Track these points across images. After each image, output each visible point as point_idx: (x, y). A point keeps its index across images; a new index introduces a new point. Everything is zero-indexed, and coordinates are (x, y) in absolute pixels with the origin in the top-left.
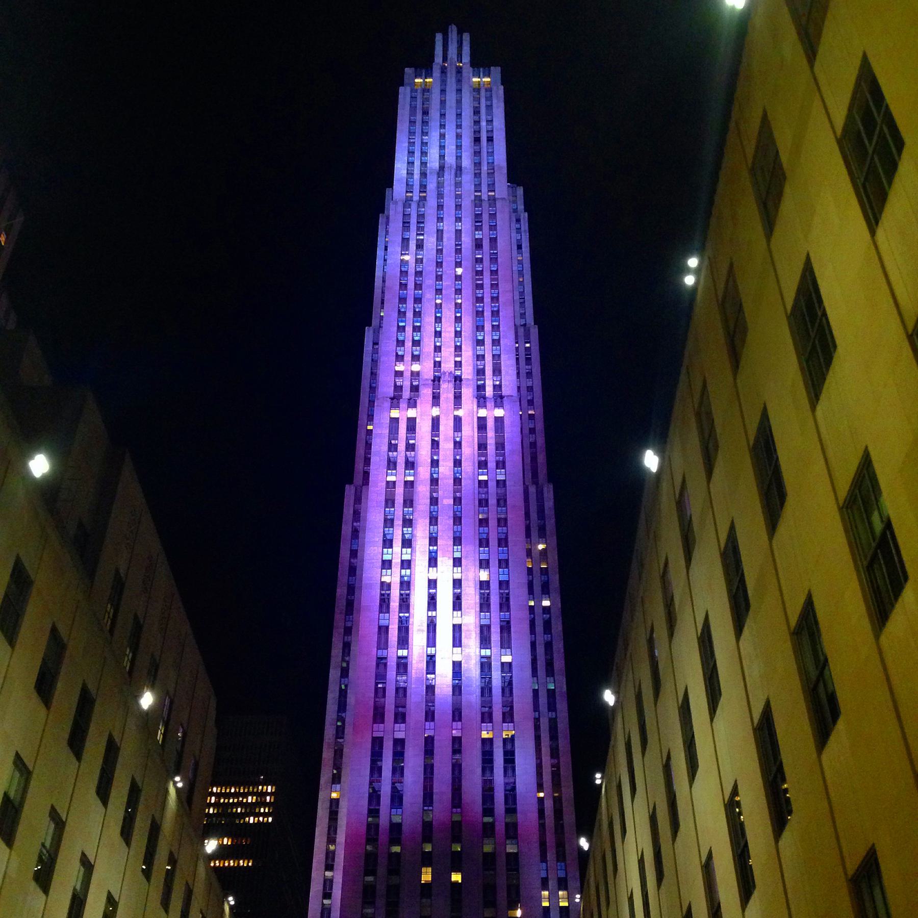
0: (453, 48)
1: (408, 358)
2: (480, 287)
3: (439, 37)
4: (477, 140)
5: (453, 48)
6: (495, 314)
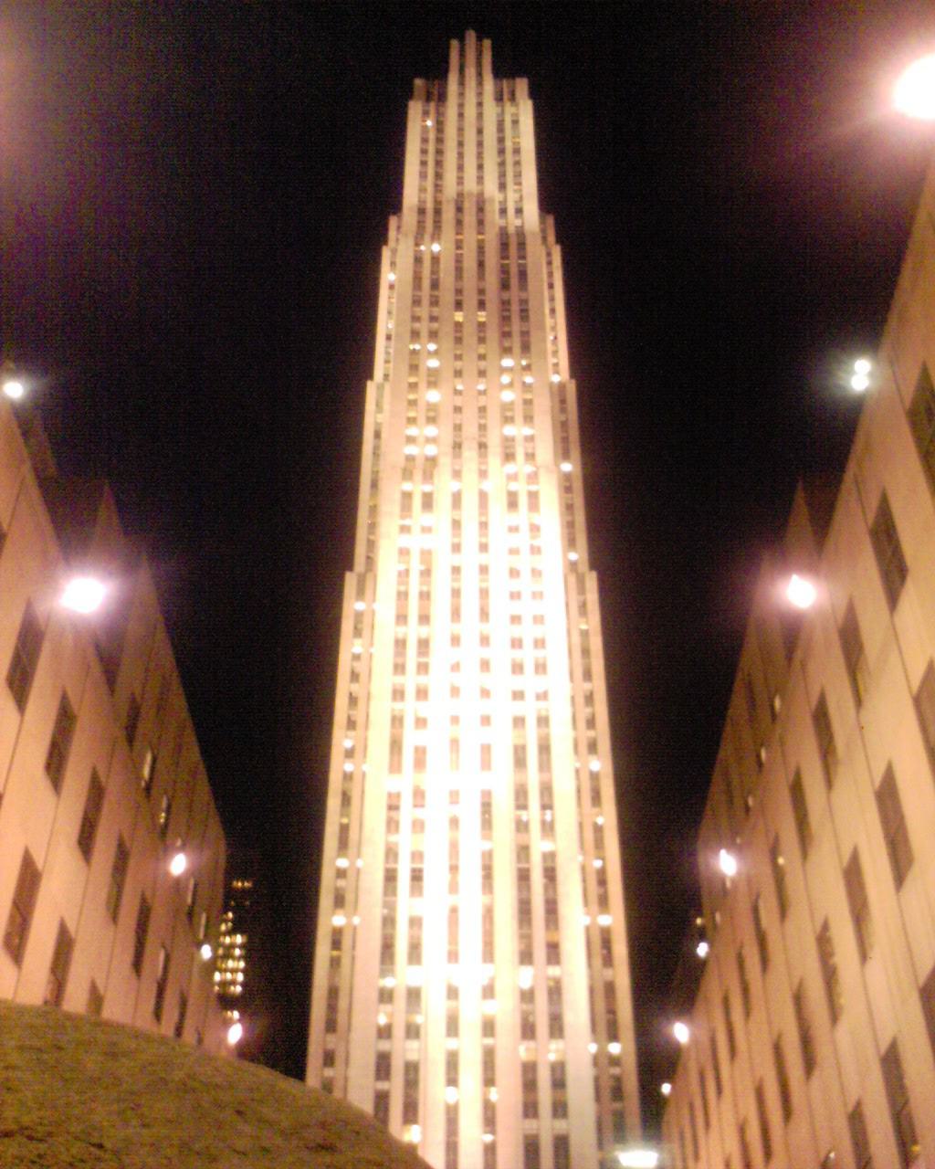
3: (455, 44)
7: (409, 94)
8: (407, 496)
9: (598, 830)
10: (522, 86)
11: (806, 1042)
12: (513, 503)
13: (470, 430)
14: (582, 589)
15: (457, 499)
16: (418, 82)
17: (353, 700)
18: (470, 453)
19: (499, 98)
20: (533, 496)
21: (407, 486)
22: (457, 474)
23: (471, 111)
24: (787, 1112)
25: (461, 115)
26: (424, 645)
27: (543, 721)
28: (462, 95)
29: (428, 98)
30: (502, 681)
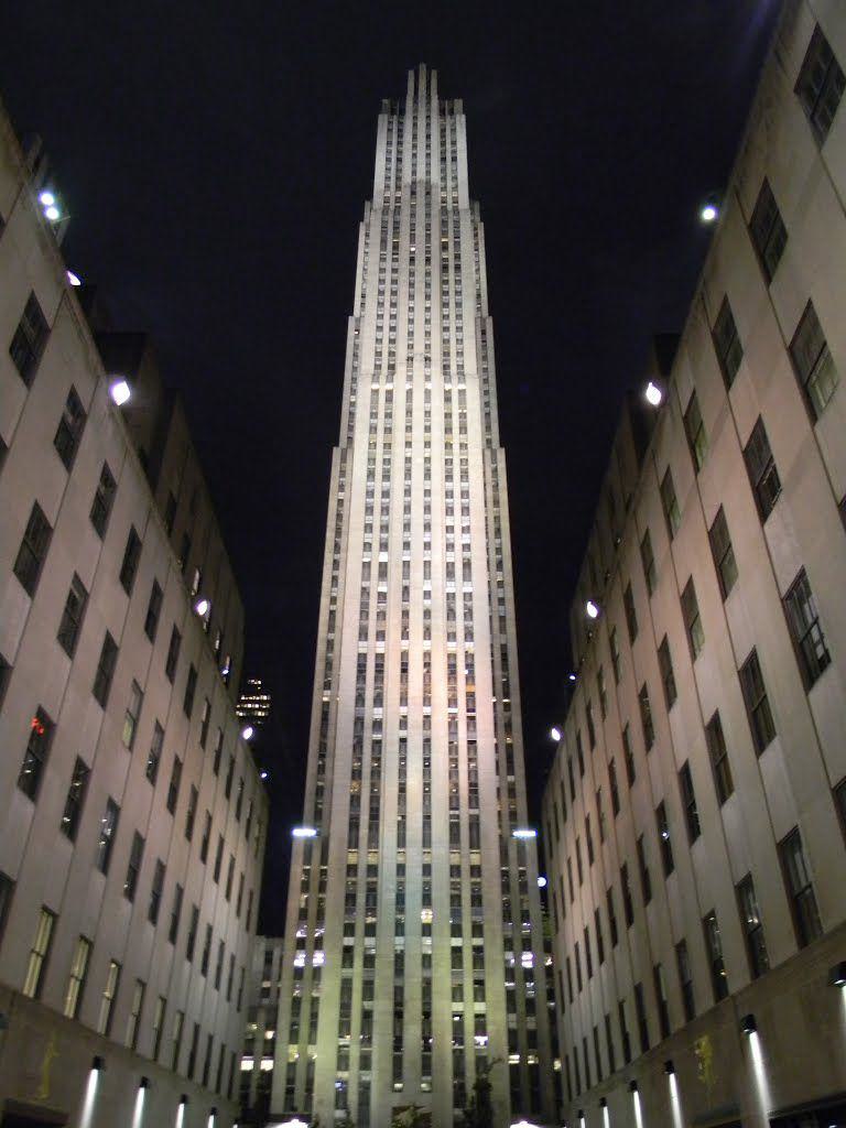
0: (422, 85)
3: (411, 74)
4: (443, 159)
5: (422, 85)
6: (458, 305)
7: (379, 110)
9: (502, 619)
10: (459, 104)
11: (648, 726)
13: (419, 348)
14: (494, 460)
15: (409, 393)
16: (385, 101)
18: (418, 364)
19: (442, 112)
22: (410, 378)
23: (422, 123)
24: (631, 778)
25: (415, 125)
28: (416, 110)
29: (393, 112)
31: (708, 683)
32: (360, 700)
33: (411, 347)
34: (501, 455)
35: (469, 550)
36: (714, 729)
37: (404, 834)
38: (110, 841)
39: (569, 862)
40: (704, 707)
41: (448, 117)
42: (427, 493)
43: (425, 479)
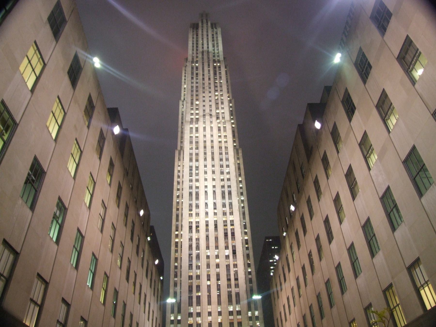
1: (194, 109)
2: (217, 86)
8: (191, 128)
12: (219, 129)
13: (207, 111)
14: (238, 153)
15: (205, 128)
17: (178, 183)
18: (208, 117)
20: (225, 128)
21: (191, 126)
22: (204, 123)
26: (197, 168)
27: (229, 187)
30: (217, 176)
31: (348, 231)
32: (190, 247)
33: (204, 111)
34: (240, 151)
35: (230, 188)
36: (351, 249)
37: (211, 300)
38: (115, 305)
39: (284, 306)
40: (347, 244)
41: (214, 29)
42: (213, 166)
43: (212, 160)
